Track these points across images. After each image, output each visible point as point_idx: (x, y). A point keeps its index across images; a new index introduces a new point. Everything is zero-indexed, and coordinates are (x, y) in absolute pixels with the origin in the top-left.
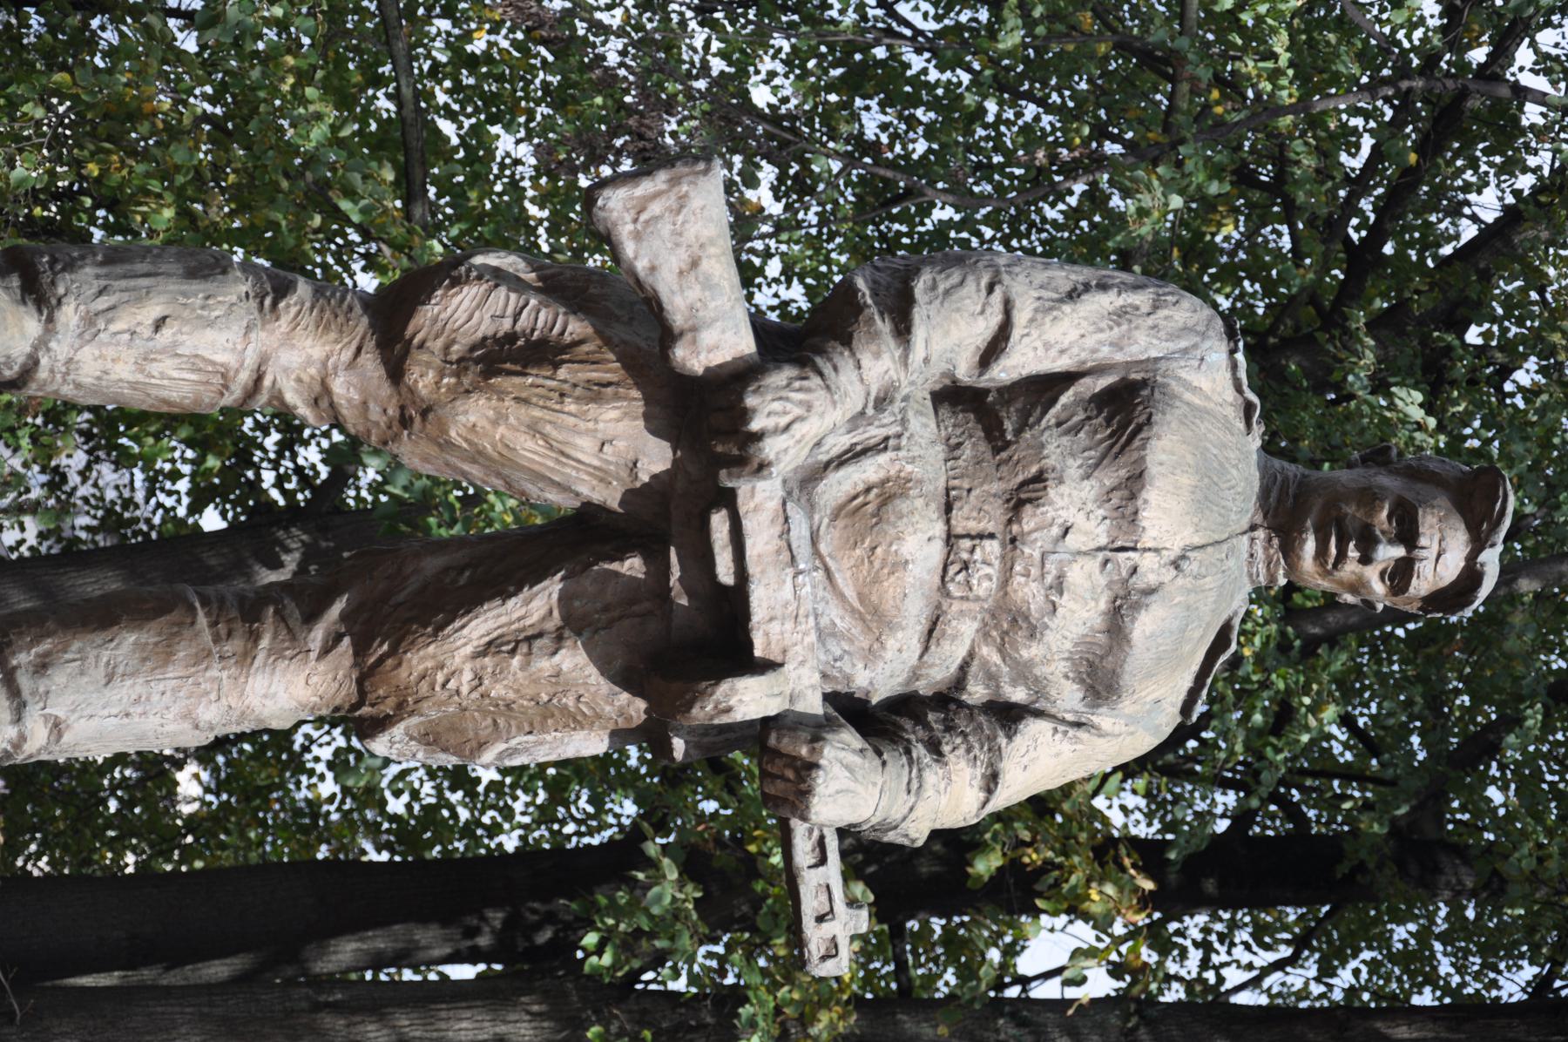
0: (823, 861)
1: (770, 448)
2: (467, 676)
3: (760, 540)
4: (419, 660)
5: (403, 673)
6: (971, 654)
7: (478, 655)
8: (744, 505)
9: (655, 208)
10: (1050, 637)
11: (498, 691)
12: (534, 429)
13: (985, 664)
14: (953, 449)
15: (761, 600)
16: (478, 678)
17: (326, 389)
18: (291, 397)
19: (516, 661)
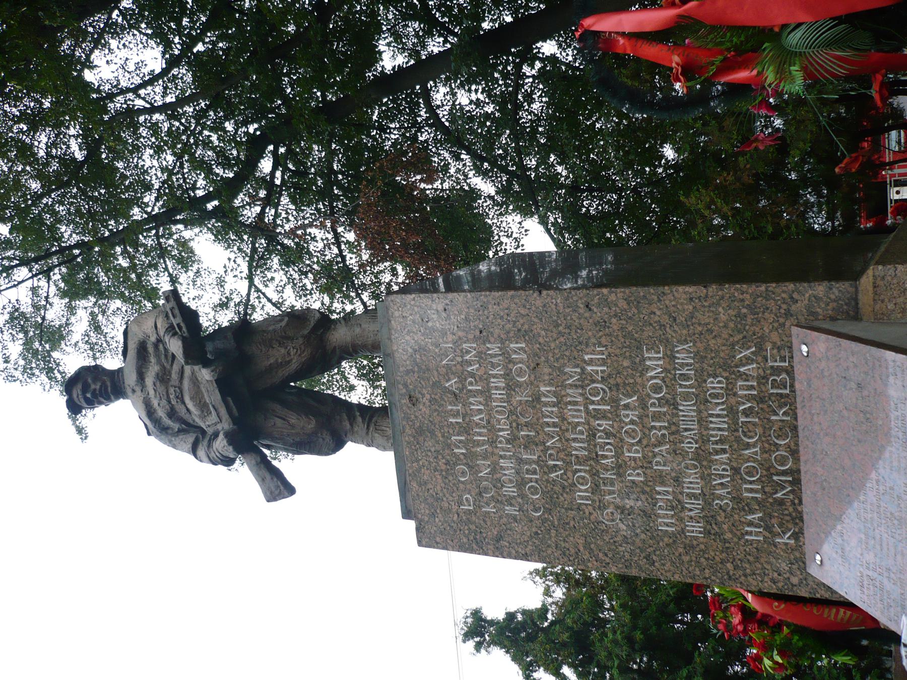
0: (178, 325)
1: (225, 442)
2: (292, 354)
3: (223, 411)
4: (306, 354)
5: (309, 351)
6: (172, 365)
7: (291, 360)
8: (229, 420)
9: (277, 492)
10: (153, 373)
11: (283, 351)
12: (293, 426)
13: (168, 362)
14: (194, 421)
15: (219, 397)
16: (289, 354)
17: (351, 425)
18: (359, 419)
19: (280, 361)
